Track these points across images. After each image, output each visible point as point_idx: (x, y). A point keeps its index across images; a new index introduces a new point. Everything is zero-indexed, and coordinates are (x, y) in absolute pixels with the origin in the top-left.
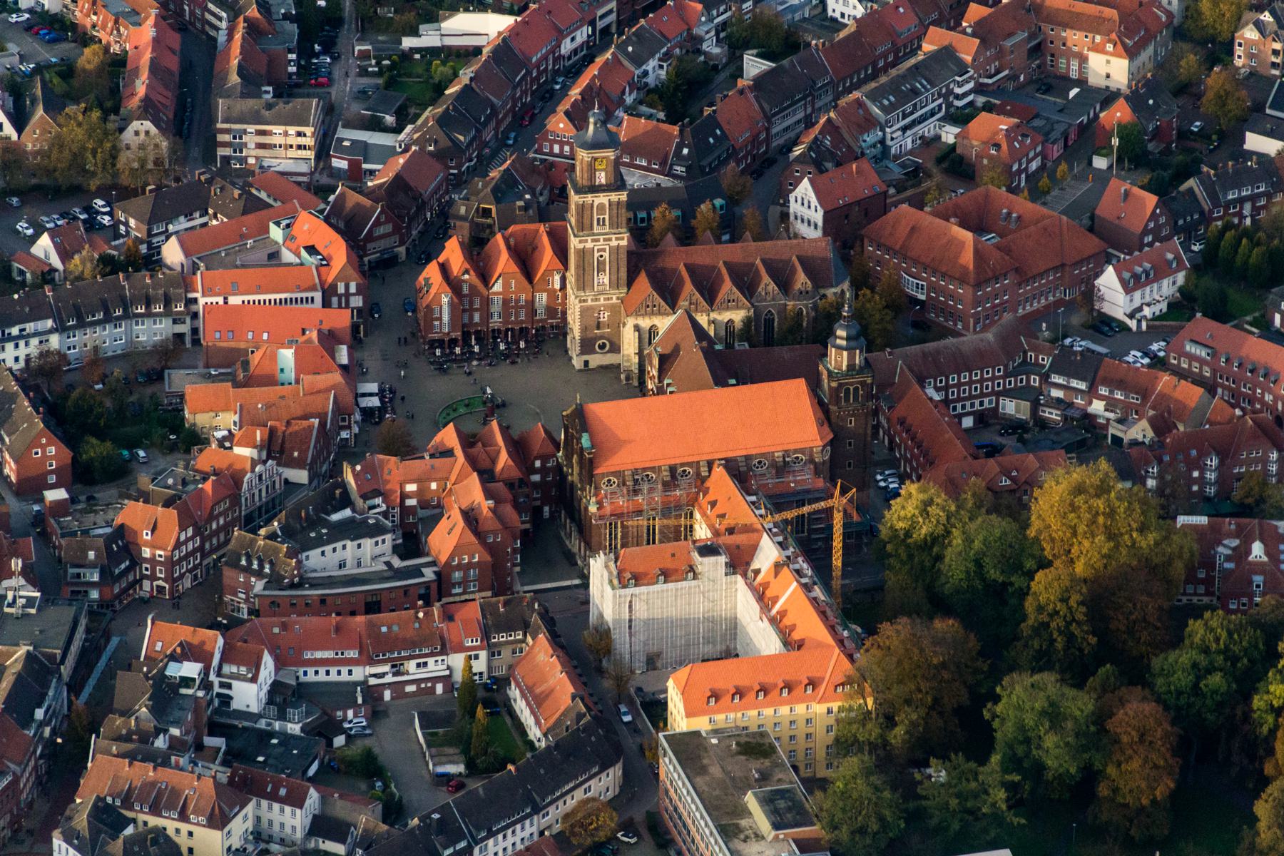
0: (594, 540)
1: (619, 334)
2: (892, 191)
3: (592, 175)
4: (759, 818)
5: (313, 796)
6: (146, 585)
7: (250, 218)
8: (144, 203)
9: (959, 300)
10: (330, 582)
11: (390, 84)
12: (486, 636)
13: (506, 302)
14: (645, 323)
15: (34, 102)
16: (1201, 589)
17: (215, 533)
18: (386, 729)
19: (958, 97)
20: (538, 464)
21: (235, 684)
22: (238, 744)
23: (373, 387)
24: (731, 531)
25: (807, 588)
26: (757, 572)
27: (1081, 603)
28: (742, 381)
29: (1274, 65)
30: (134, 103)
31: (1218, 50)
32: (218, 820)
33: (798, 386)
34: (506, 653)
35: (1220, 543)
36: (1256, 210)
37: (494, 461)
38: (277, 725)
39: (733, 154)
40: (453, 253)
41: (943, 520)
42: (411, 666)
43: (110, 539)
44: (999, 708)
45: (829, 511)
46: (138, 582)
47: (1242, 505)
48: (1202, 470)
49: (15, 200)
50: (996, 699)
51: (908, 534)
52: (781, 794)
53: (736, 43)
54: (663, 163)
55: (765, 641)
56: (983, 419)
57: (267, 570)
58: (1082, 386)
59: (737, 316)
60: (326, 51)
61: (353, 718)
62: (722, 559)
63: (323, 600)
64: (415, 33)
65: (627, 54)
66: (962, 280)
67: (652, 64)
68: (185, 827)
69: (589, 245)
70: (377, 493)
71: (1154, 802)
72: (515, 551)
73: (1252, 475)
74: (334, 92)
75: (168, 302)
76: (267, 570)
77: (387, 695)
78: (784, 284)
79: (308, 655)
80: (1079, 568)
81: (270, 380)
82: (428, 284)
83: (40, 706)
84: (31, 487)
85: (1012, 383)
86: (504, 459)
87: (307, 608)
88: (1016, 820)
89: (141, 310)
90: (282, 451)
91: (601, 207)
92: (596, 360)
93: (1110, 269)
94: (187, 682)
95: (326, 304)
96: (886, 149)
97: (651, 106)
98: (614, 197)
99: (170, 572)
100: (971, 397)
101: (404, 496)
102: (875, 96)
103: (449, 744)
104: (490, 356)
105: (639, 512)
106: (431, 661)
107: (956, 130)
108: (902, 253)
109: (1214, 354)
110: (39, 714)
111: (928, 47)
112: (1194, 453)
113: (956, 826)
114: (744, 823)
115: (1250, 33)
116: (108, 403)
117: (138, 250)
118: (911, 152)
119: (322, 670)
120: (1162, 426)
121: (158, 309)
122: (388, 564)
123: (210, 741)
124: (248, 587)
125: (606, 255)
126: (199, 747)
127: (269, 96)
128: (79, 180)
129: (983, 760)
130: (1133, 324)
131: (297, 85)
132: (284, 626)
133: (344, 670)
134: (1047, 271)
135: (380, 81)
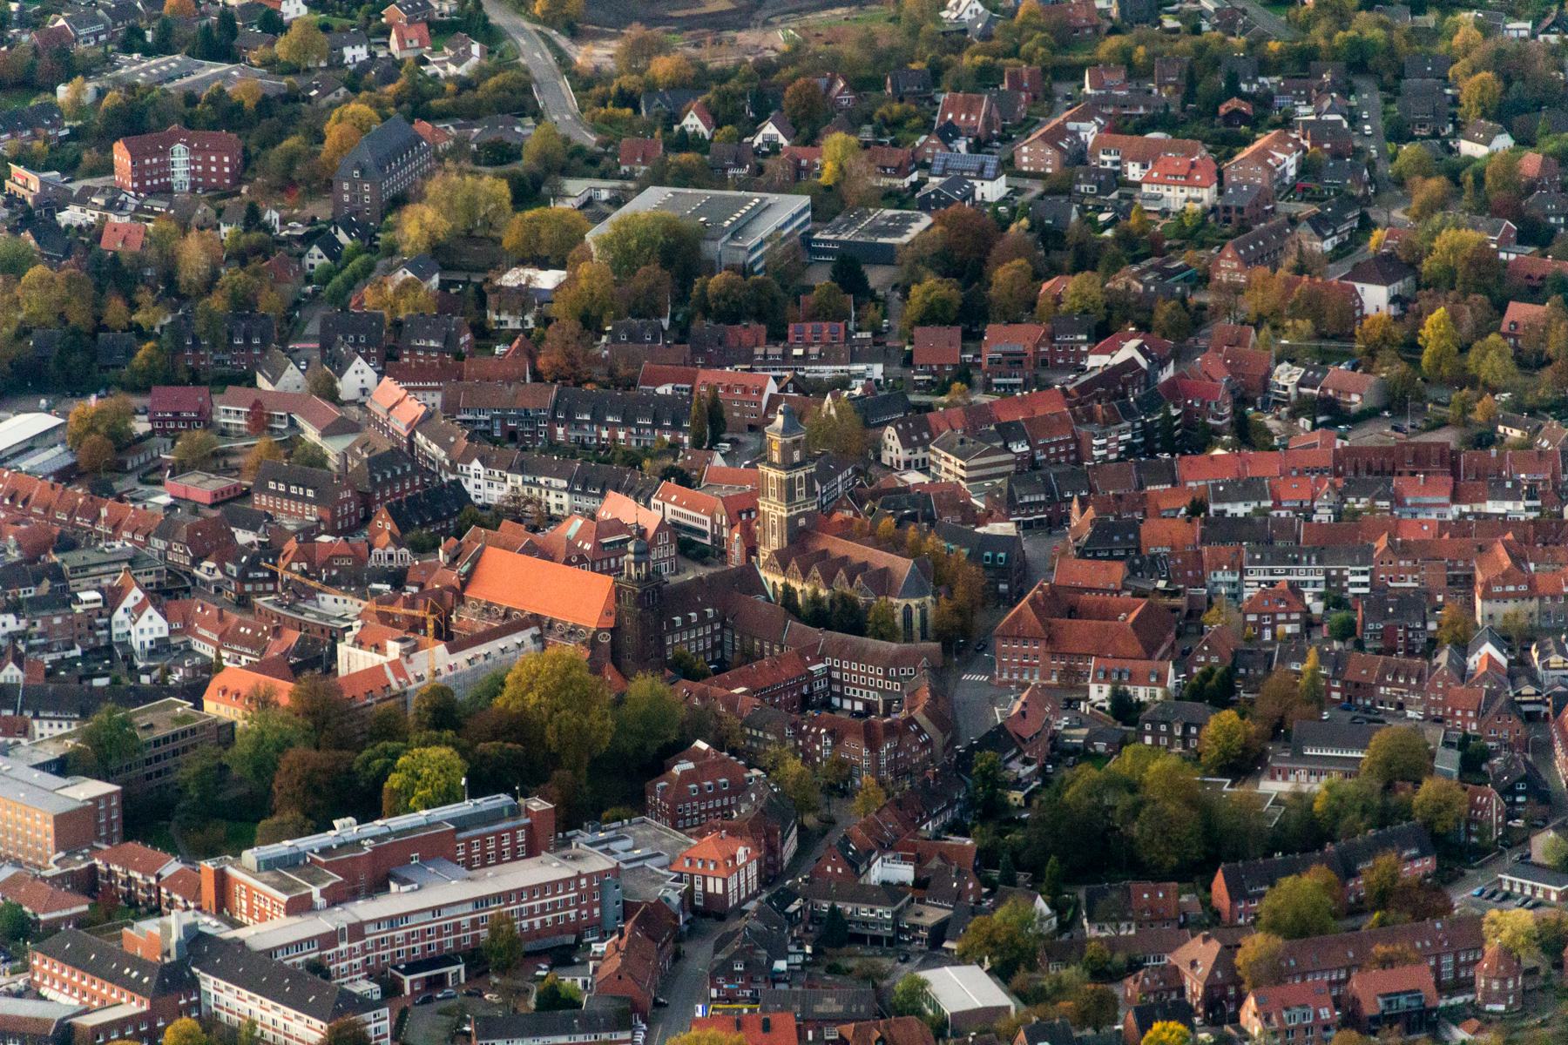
132: (203, 610)
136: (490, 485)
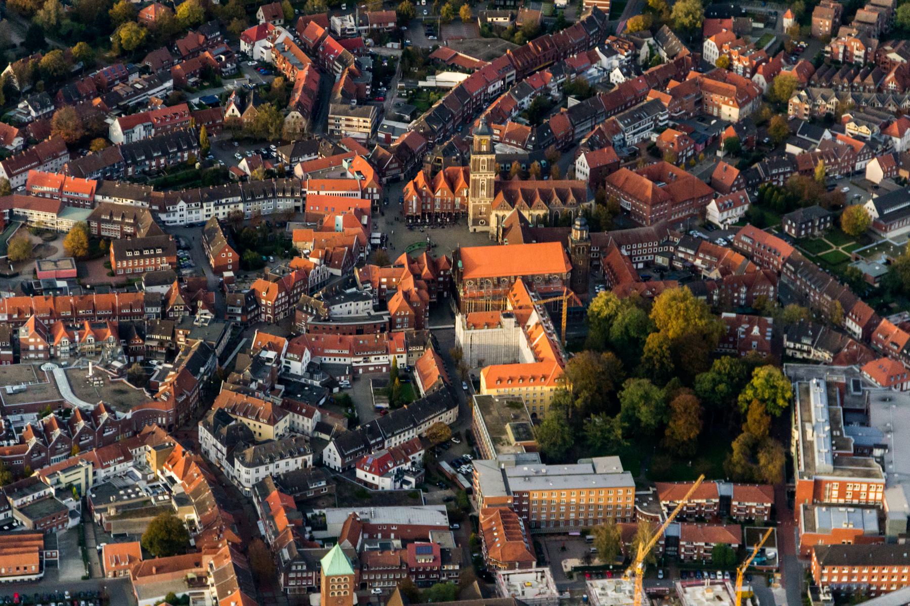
0: (462, 308)
1: (489, 218)
2: (622, 161)
3: (480, 147)
4: (511, 436)
5: (317, 414)
6: (263, 316)
7: (336, 157)
8: (290, 148)
9: (644, 211)
10: (342, 319)
11: (409, 102)
12: (407, 348)
13: (442, 201)
14: (500, 213)
15: (249, 101)
16: (731, 346)
17: (294, 295)
18: (358, 386)
19: (661, 121)
20: (442, 273)
21: (292, 362)
22: (290, 389)
23: (378, 235)
24: (520, 308)
25: (550, 335)
26: (529, 326)
27: (667, 349)
28: (539, 241)
29: (806, 115)
30: (293, 104)
31: (782, 107)
32: (273, 421)
33: (558, 245)
34: (415, 356)
35: (740, 326)
36: (785, 178)
37: (422, 271)
38: (309, 381)
39: (555, 141)
40: (420, 178)
41: (615, 308)
42: (372, 358)
43: (248, 295)
44: (623, 393)
45: (562, 301)
46: (259, 315)
47: (755, 309)
48: (739, 292)
49: (236, 144)
50: (623, 389)
51: (599, 314)
52: (522, 425)
53: (566, 91)
54: (523, 143)
55: (528, 357)
56: (648, 264)
57: (314, 312)
58: (692, 252)
59: (541, 213)
60: (384, 86)
61: (344, 381)
62: (513, 320)
63: (337, 328)
64: (425, 80)
65: (515, 94)
66: (646, 203)
67: (526, 99)
68: (258, 424)
69: (478, 178)
70: (368, 281)
71: (689, 439)
72: (426, 311)
73: (760, 296)
74: (385, 104)
75: (293, 192)
76: (314, 312)
77: (361, 371)
78: (564, 200)
79: (326, 351)
80: (671, 334)
81: (331, 229)
82: (407, 191)
83: (203, 366)
84: (218, 271)
85: (661, 249)
86: (426, 270)
87: (330, 330)
88: (626, 444)
89: (281, 195)
90: (330, 261)
91: (483, 162)
92: (479, 228)
93: (713, 201)
94: (269, 360)
95: (363, 197)
96: (625, 143)
97: (524, 117)
98: (490, 157)
99: (274, 311)
100: (642, 254)
101: (380, 284)
102: (621, 119)
103: (384, 394)
104: (434, 224)
105: (482, 297)
106: (381, 357)
107: (657, 135)
108: (621, 189)
109: (754, 242)
110: (202, 370)
111: (649, 98)
112: (736, 285)
113: (599, 444)
114: (503, 437)
115: (796, 100)
116: (259, 235)
117: (283, 169)
118: (636, 145)
119: (332, 359)
120: (724, 272)
121: (288, 195)
122: (369, 313)
123: (278, 386)
124: (306, 319)
125: (485, 182)
126: (273, 389)
127: (354, 104)
128: (265, 136)
129: (613, 416)
130: (722, 226)
131: (370, 100)
132: (317, 338)
133: (342, 359)
134: (686, 201)
135: (406, 100)
136: (190, 213)
